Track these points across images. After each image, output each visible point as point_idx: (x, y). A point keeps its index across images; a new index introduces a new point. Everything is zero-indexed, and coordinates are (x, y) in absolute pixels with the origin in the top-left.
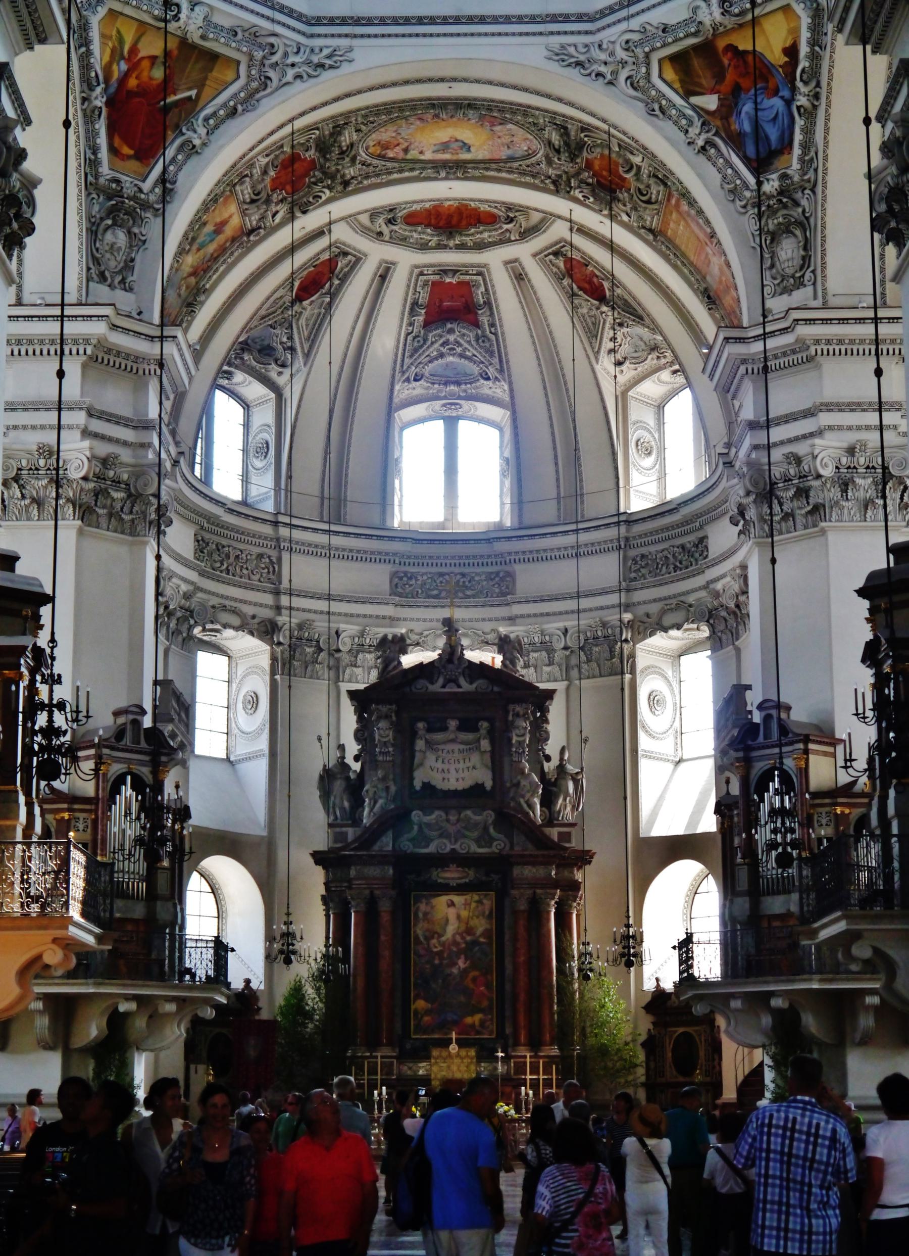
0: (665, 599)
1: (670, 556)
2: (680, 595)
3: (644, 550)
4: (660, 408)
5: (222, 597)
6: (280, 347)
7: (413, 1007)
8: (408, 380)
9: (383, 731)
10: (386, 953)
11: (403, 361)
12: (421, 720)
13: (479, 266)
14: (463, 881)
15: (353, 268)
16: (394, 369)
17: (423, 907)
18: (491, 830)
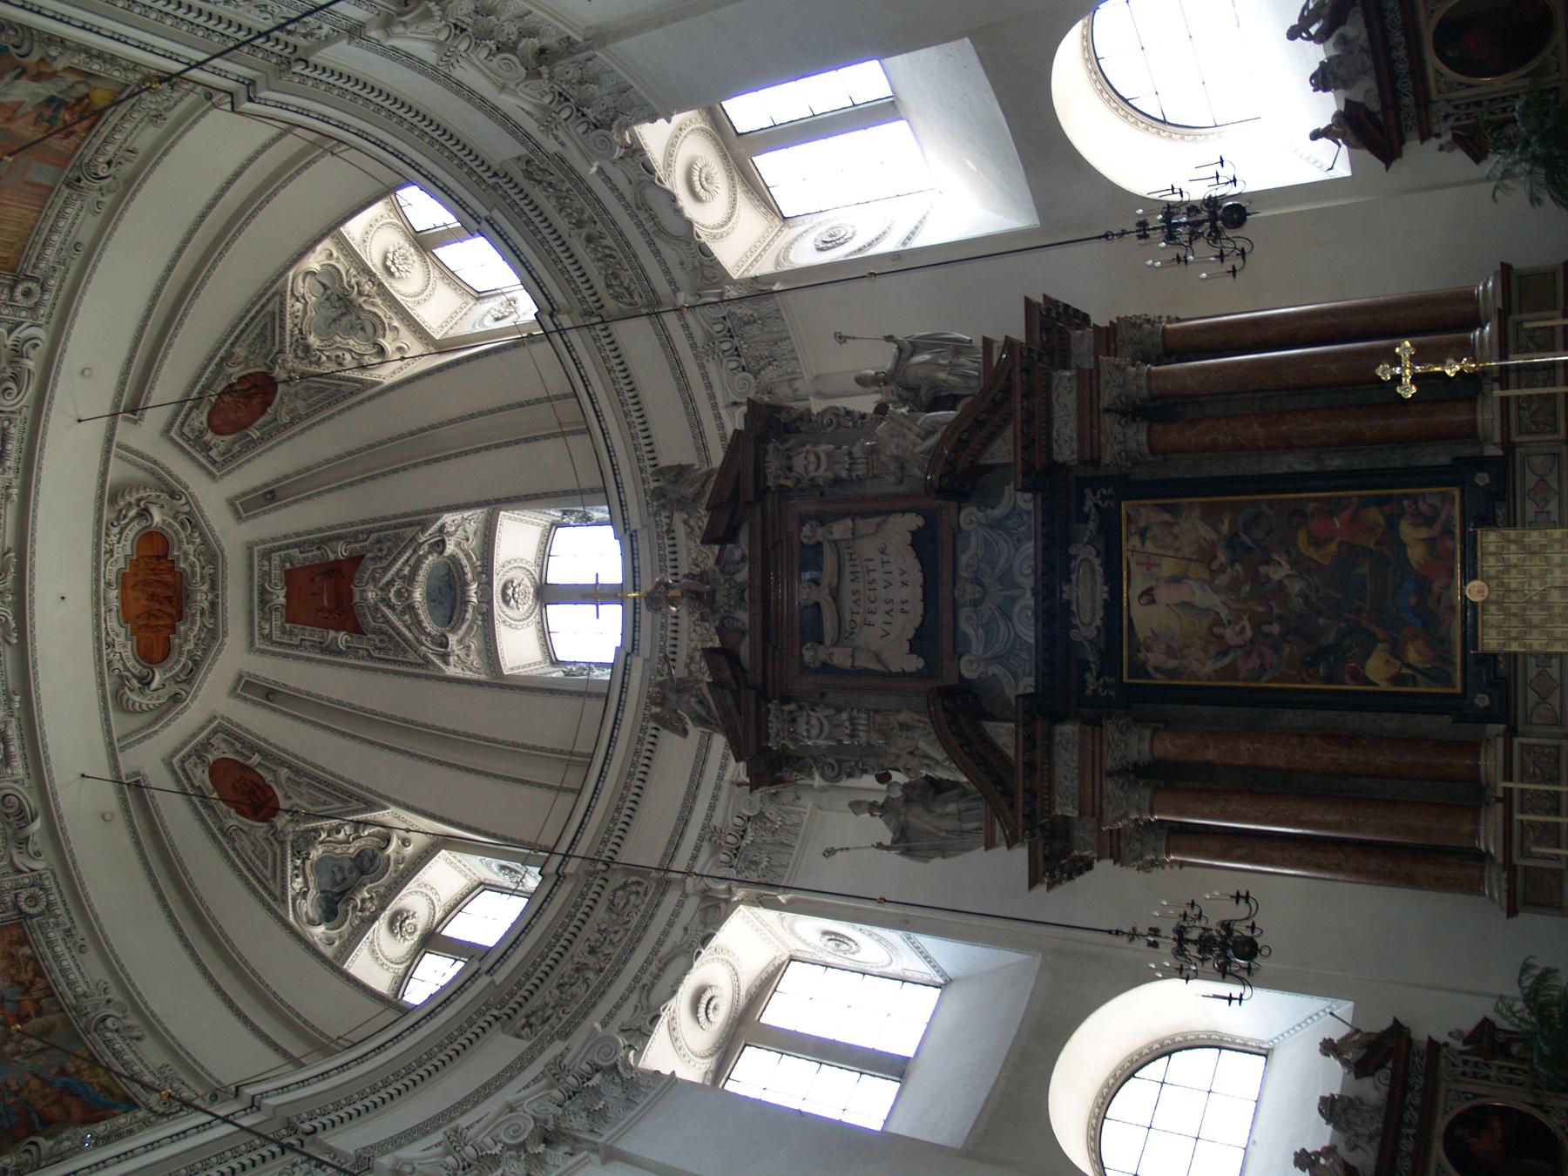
0: (645, 233)
1: (585, 232)
2: (627, 206)
3: (599, 284)
4: (479, 296)
5: (631, 989)
6: (357, 844)
7: (1384, 686)
8: (445, 657)
9: (813, 731)
10: (1245, 751)
11: (411, 664)
12: (802, 656)
13: (251, 557)
14: (1099, 570)
15: (238, 738)
16: (417, 676)
17: (1155, 658)
18: (998, 512)
